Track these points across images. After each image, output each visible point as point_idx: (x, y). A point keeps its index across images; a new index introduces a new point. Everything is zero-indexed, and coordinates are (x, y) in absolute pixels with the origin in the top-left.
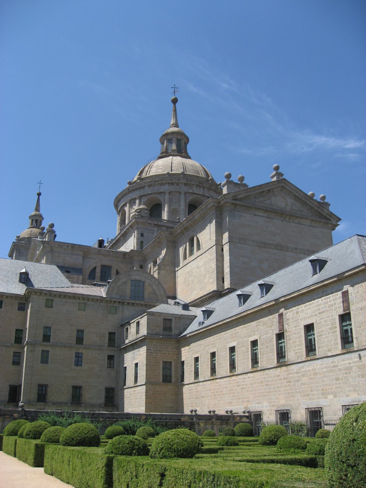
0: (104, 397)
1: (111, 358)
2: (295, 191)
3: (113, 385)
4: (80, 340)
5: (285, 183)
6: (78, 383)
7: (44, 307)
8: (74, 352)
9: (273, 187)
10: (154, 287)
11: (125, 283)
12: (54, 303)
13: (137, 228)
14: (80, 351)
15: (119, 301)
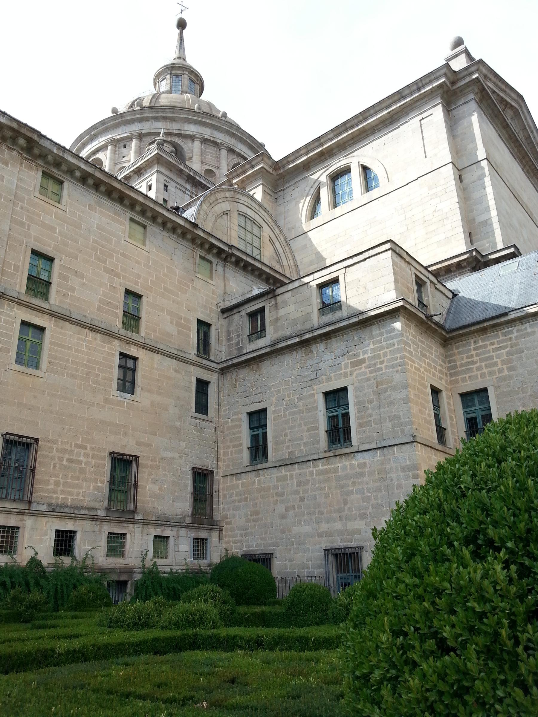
0: (189, 496)
1: (202, 386)
2: (530, 127)
3: (209, 464)
4: (132, 319)
5: (521, 107)
6: (128, 447)
7: (37, 194)
8: (117, 347)
9: (513, 104)
10: (277, 244)
11: (226, 213)
12: (65, 192)
13: (157, 171)
14: (133, 351)
15: (222, 246)
